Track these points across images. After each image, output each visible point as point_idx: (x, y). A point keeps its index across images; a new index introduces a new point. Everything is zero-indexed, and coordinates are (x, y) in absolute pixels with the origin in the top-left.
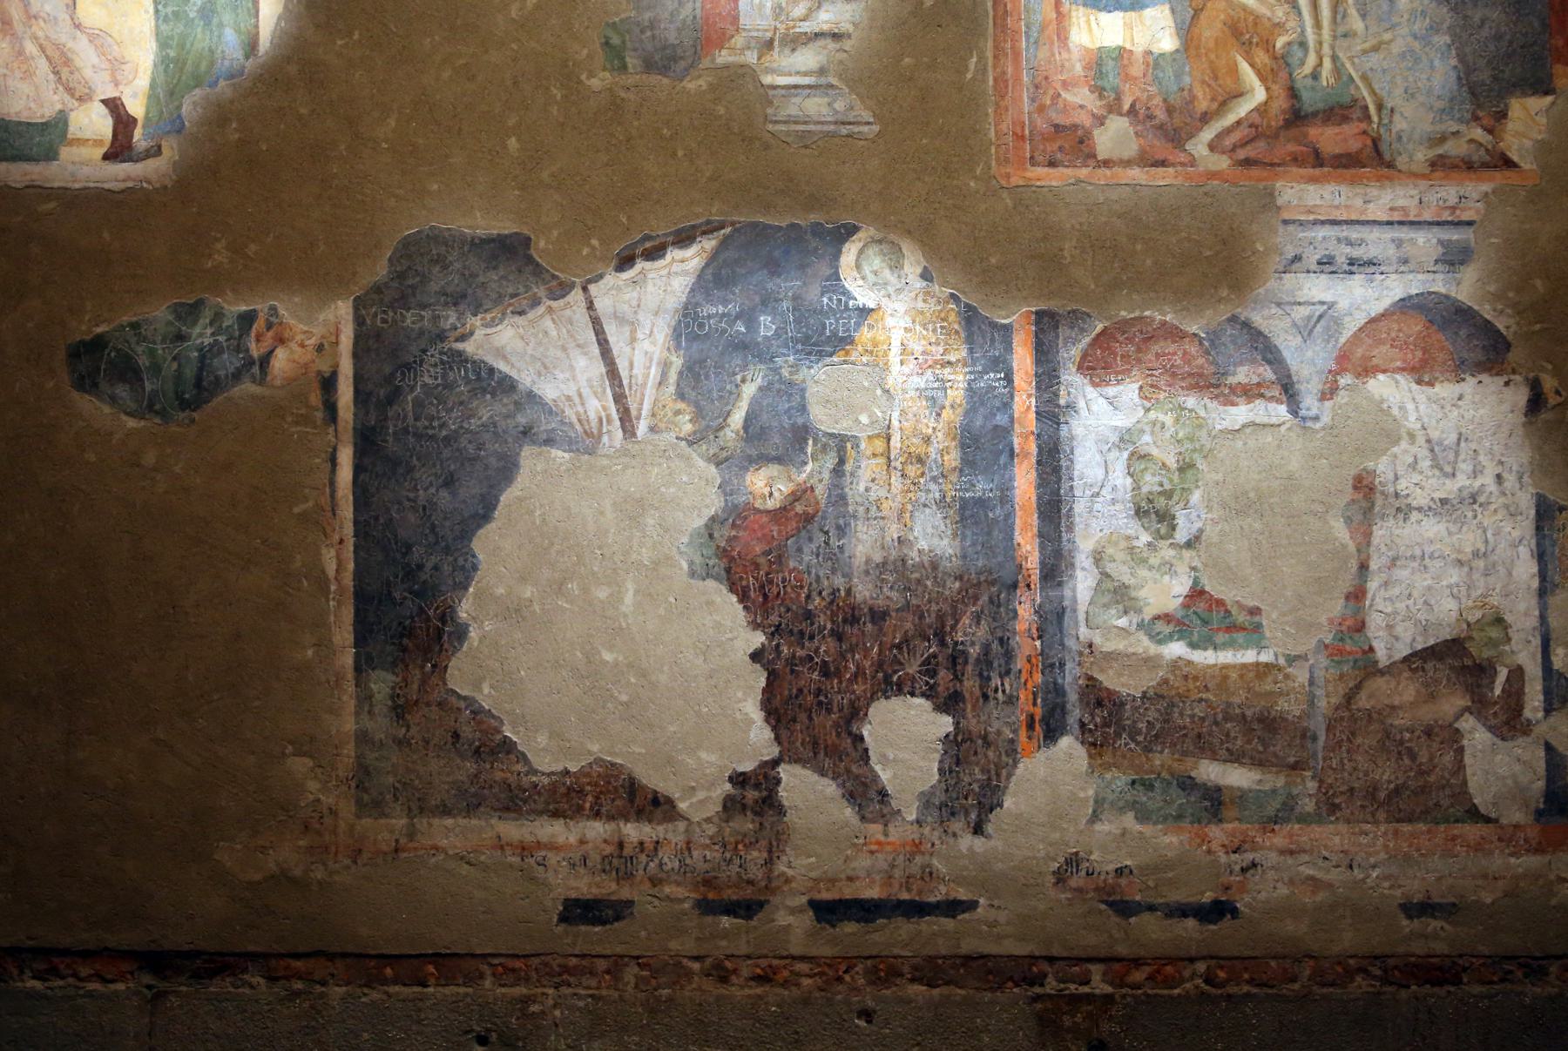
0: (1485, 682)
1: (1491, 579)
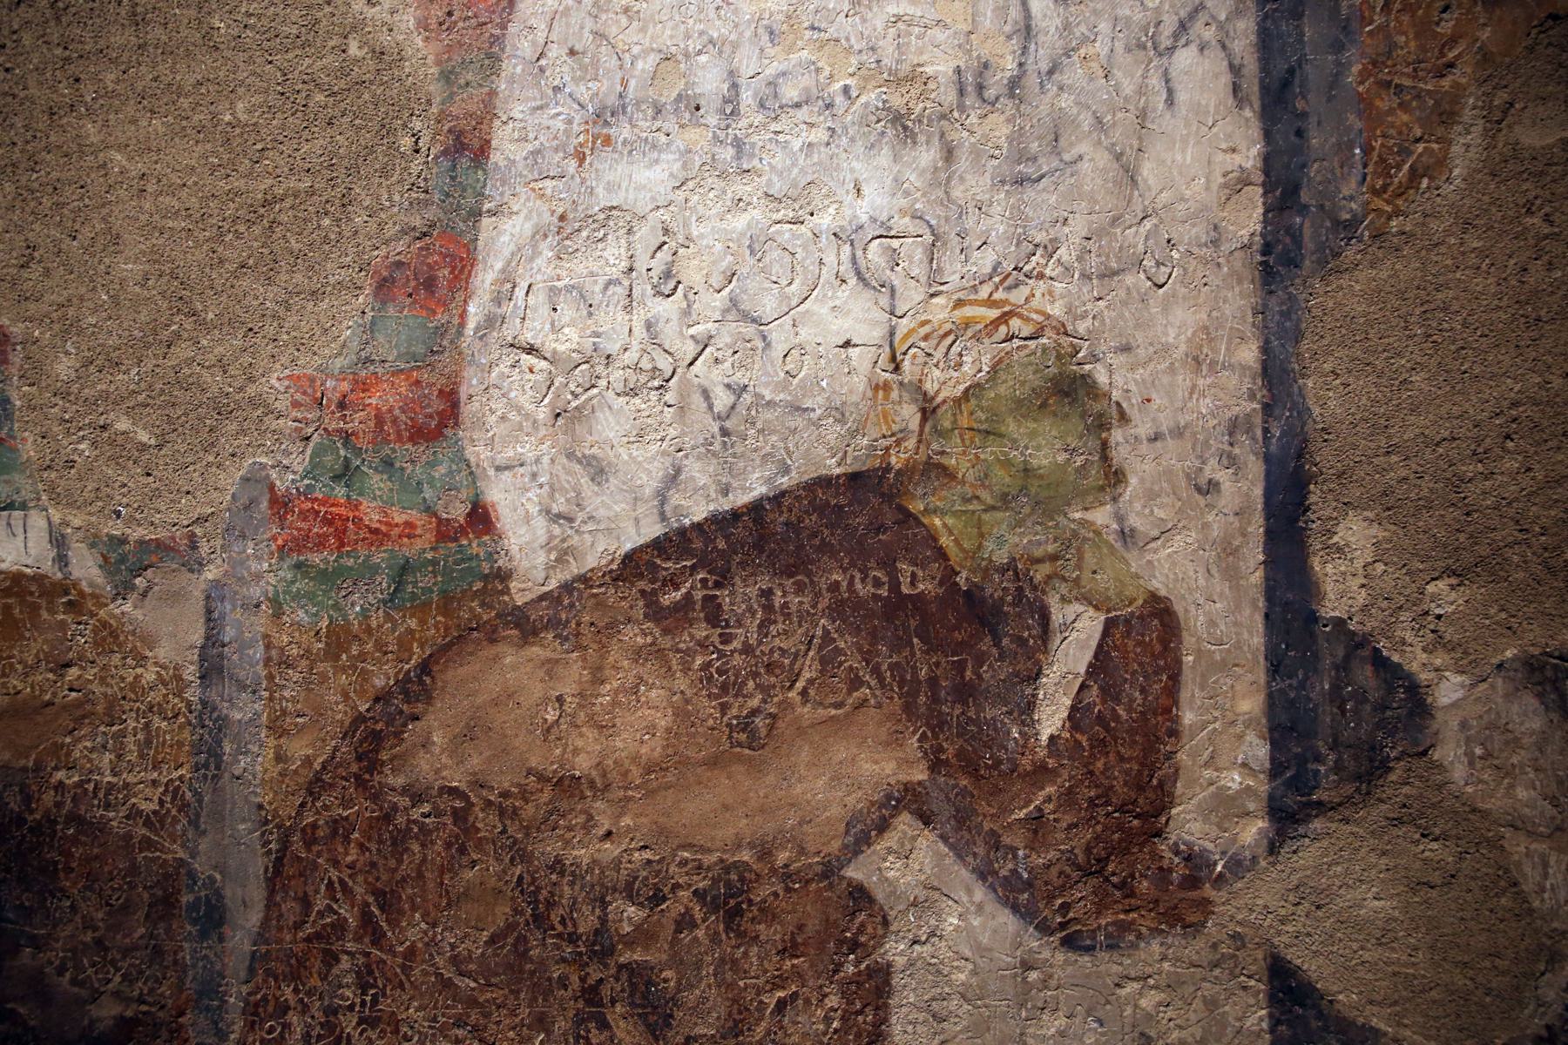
0: (994, 673)
1: (1043, 201)
